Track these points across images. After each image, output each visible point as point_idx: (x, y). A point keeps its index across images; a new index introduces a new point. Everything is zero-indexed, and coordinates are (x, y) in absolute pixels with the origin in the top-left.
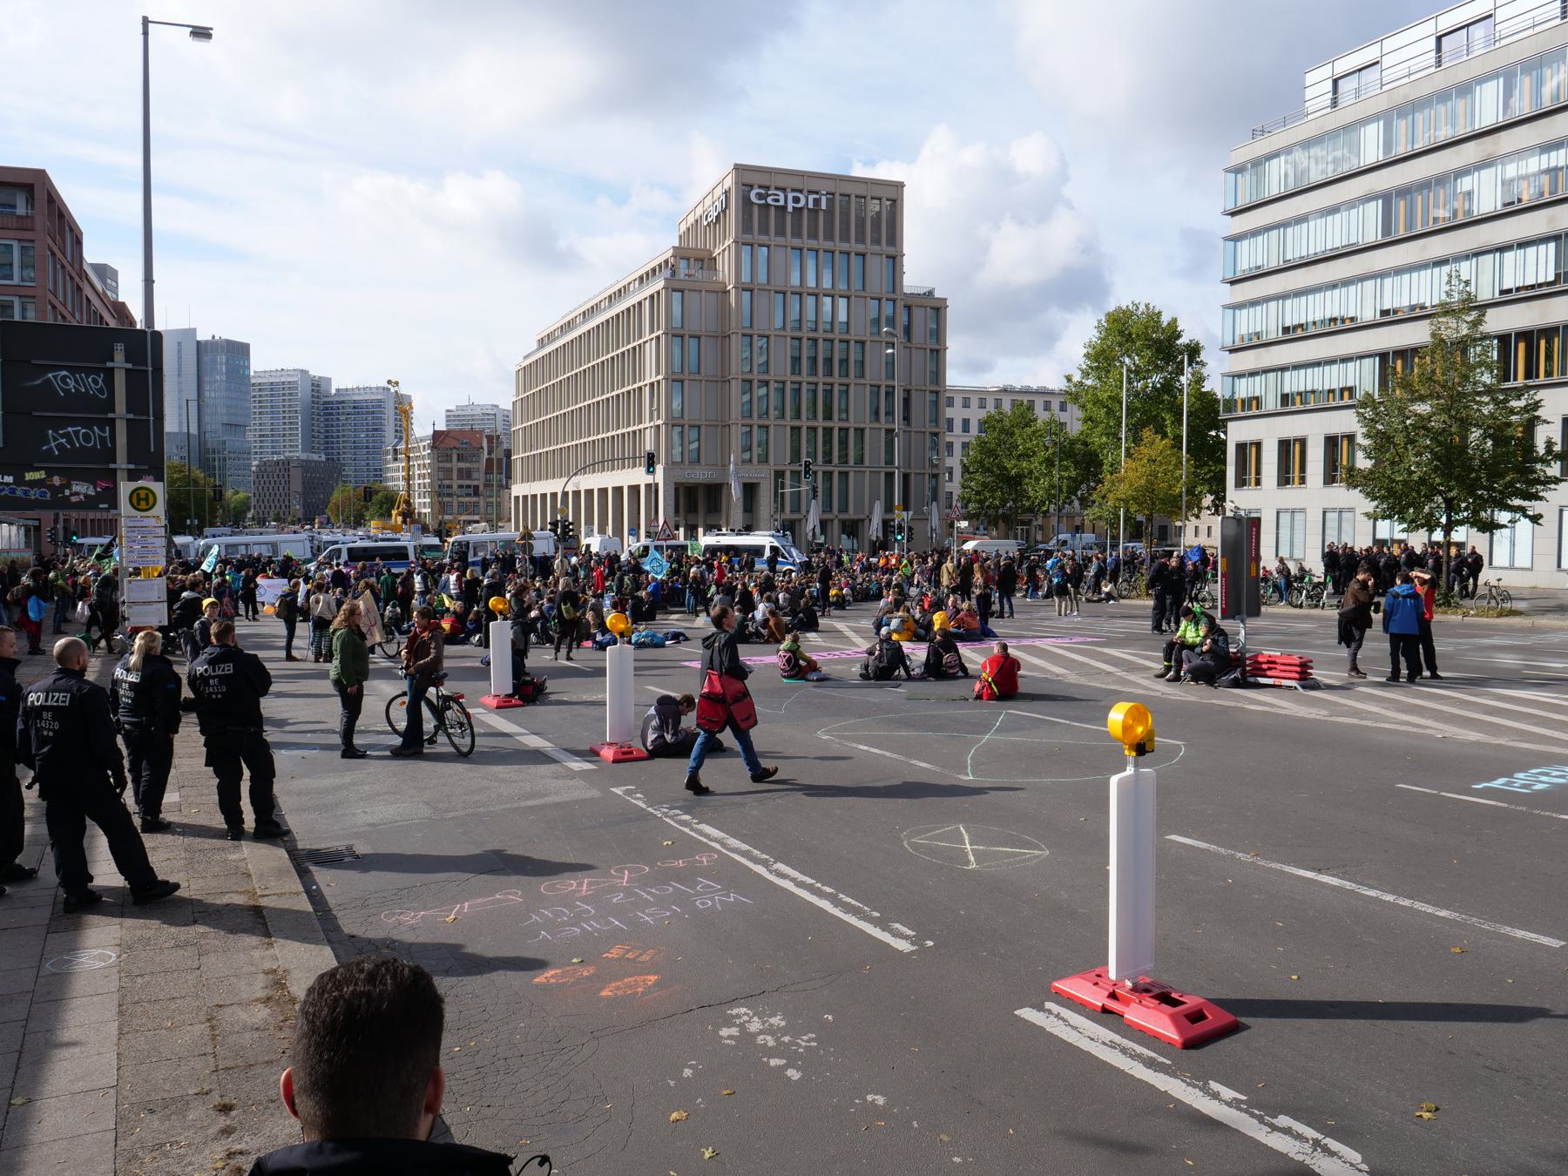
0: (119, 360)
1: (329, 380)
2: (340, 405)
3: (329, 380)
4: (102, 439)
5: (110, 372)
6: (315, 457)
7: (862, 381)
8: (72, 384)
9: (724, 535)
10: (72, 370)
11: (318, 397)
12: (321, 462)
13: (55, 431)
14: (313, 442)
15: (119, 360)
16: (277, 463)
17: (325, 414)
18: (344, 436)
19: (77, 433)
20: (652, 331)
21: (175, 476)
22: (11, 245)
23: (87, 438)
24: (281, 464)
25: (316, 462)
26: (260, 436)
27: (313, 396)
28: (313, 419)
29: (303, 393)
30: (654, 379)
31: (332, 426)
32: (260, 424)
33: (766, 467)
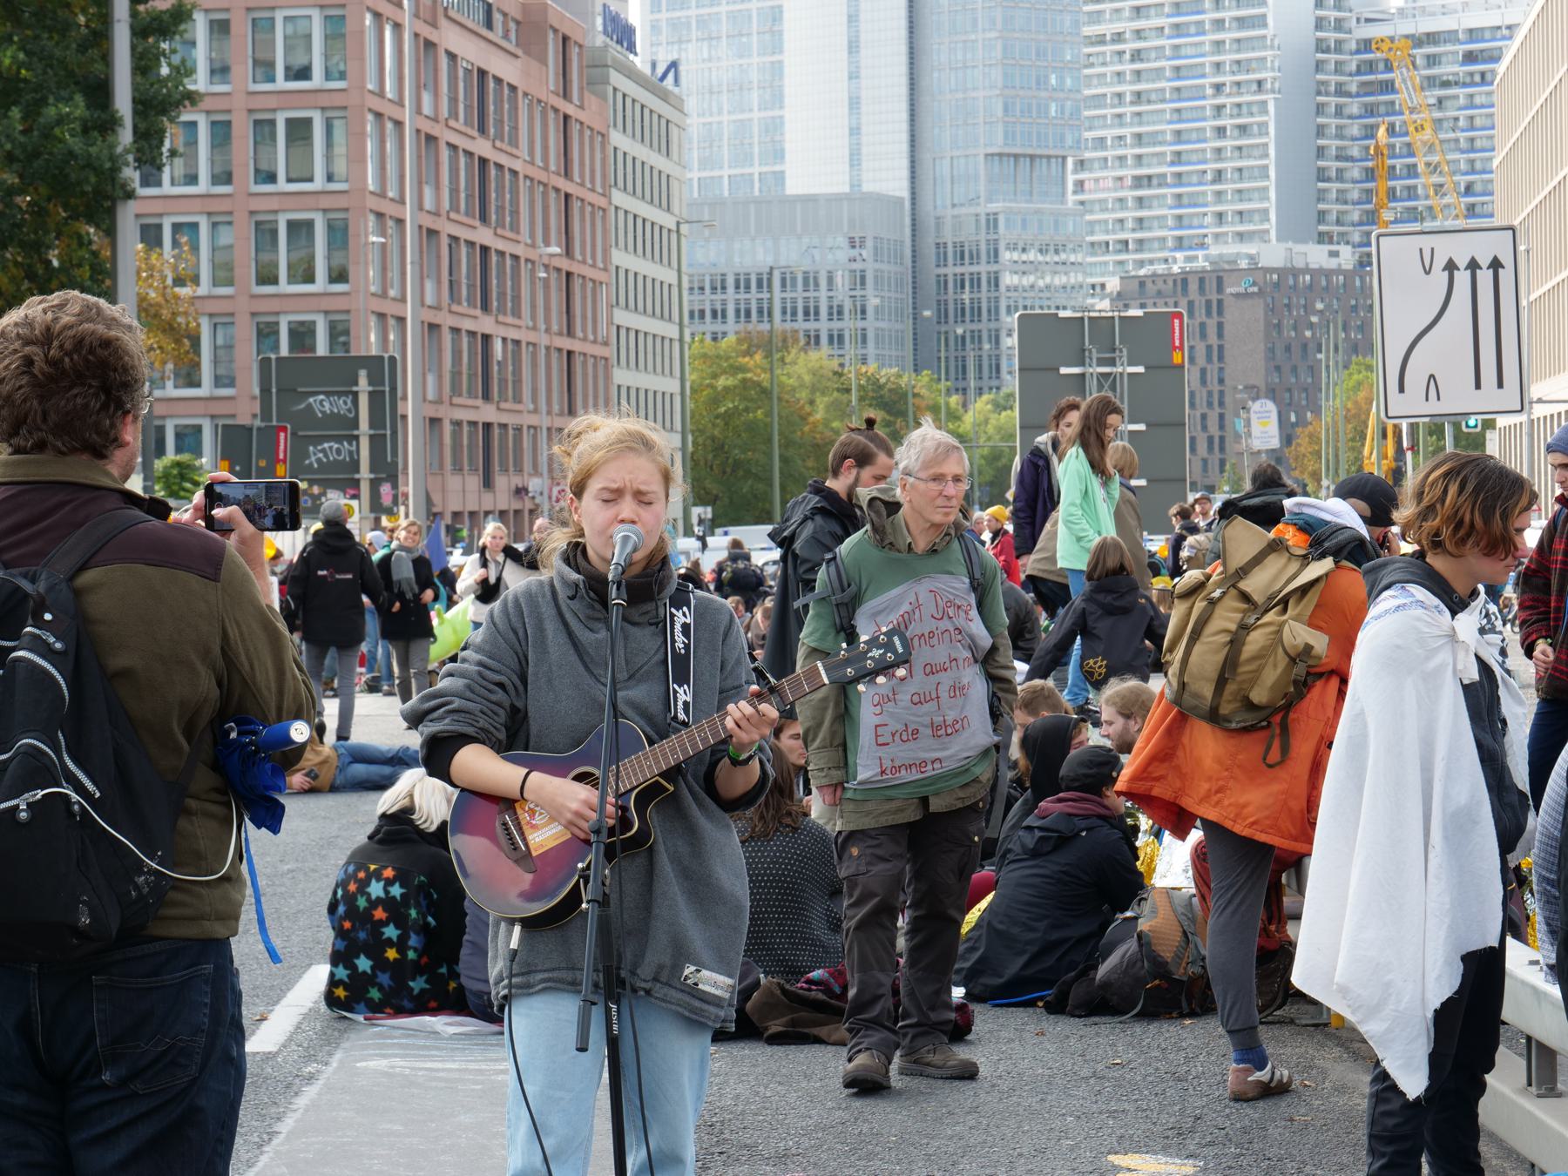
0: (363, 385)
4: (351, 453)
5: (355, 395)
6: (1316, 256)
8: (326, 404)
10: (328, 394)
11: (1339, 25)
12: (1339, 271)
13: (315, 447)
14: (1321, 196)
15: (363, 385)
16: (1183, 281)
17: (1367, 89)
19: (331, 448)
21: (722, 382)
22: (310, 17)
23: (338, 452)
24: (1193, 286)
26: (1139, 182)
27: (1320, 24)
28: (1320, 109)
32: (1139, 136)
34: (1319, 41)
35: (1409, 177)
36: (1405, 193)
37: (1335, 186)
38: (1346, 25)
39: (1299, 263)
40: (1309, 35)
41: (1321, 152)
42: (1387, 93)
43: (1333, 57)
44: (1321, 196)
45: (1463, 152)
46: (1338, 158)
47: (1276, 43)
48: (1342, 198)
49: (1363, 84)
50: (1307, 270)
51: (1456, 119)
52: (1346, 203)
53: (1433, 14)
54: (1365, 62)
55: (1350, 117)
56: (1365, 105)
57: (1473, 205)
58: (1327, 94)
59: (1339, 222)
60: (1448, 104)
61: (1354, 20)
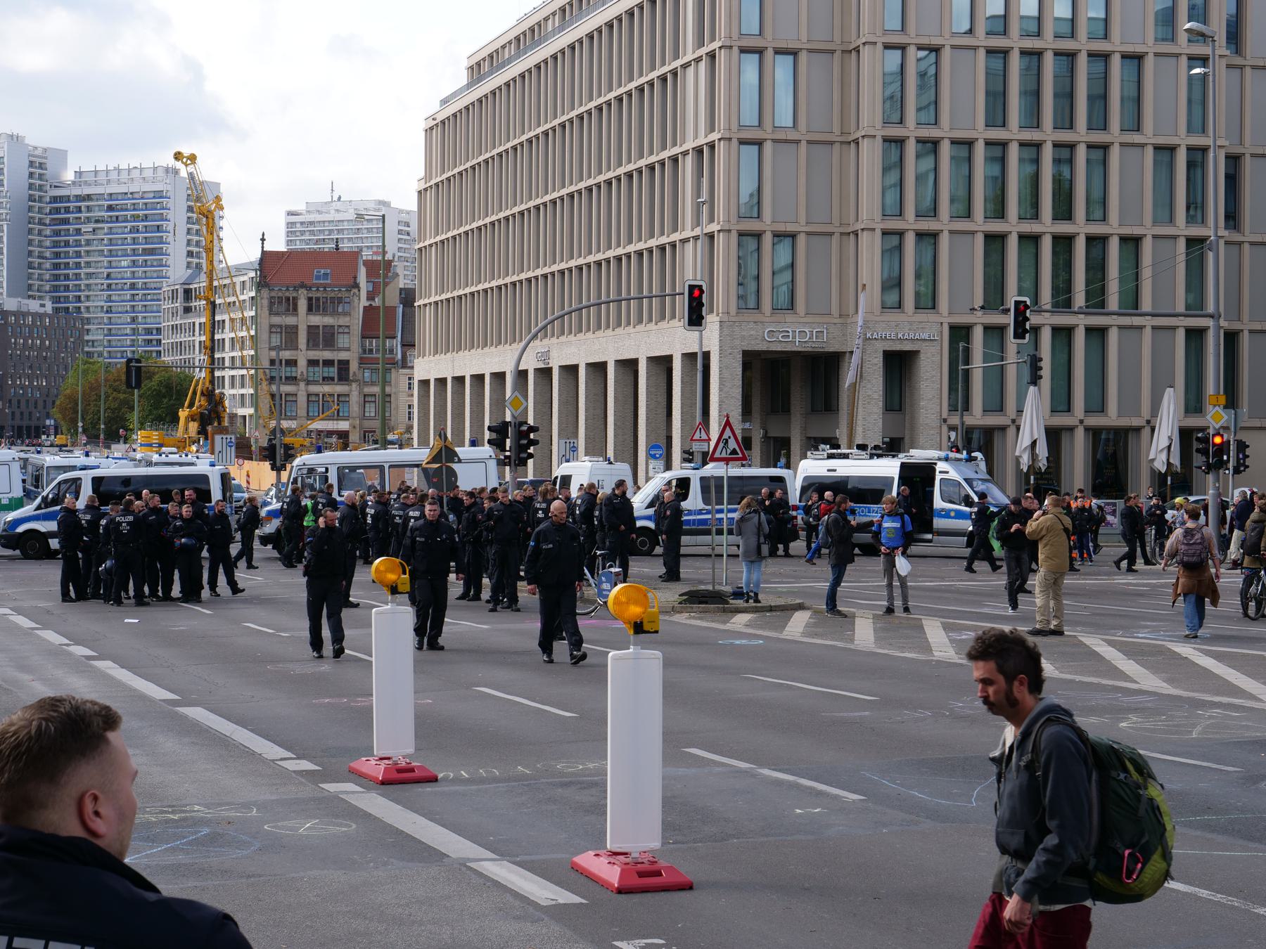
1: (62, 155)
2: (83, 204)
3: (62, 155)
6: (34, 306)
7: (1136, 138)
9: (845, 456)
11: (41, 188)
12: (45, 314)
14: (30, 277)
18: (88, 264)
20: (701, 43)
25: (36, 315)
27: (31, 186)
28: (30, 231)
29: (16, 177)
30: (701, 141)
31: (67, 244)
33: (931, 317)
34: (30, 195)
35: (76, 268)
36: (74, 277)
37: (37, 271)
38: (44, 188)
39: (24, 309)
40: (26, 193)
41: (30, 253)
42: (66, 224)
43: (37, 204)
44: (30, 277)
45: (106, 257)
46: (39, 257)
47: (8, 194)
48: (40, 278)
49: (53, 219)
50: (29, 313)
51: (103, 239)
52: (42, 281)
53: (90, 185)
54: (54, 208)
55: (45, 236)
56: (53, 230)
57: (111, 284)
58: (34, 224)
59: (38, 291)
60: (97, 231)
61: (49, 186)
